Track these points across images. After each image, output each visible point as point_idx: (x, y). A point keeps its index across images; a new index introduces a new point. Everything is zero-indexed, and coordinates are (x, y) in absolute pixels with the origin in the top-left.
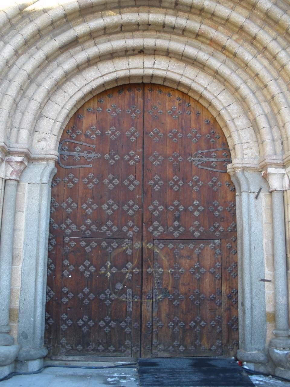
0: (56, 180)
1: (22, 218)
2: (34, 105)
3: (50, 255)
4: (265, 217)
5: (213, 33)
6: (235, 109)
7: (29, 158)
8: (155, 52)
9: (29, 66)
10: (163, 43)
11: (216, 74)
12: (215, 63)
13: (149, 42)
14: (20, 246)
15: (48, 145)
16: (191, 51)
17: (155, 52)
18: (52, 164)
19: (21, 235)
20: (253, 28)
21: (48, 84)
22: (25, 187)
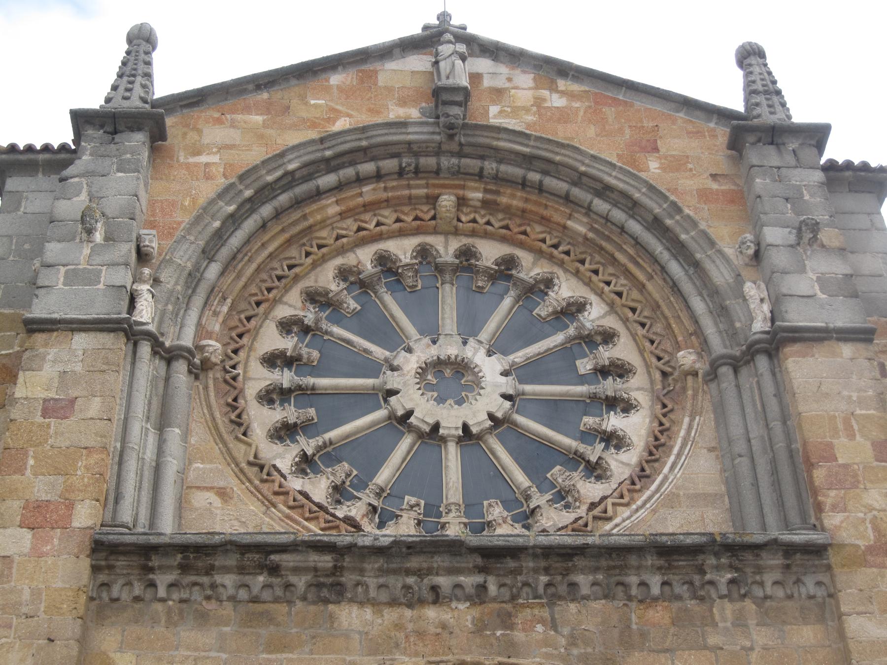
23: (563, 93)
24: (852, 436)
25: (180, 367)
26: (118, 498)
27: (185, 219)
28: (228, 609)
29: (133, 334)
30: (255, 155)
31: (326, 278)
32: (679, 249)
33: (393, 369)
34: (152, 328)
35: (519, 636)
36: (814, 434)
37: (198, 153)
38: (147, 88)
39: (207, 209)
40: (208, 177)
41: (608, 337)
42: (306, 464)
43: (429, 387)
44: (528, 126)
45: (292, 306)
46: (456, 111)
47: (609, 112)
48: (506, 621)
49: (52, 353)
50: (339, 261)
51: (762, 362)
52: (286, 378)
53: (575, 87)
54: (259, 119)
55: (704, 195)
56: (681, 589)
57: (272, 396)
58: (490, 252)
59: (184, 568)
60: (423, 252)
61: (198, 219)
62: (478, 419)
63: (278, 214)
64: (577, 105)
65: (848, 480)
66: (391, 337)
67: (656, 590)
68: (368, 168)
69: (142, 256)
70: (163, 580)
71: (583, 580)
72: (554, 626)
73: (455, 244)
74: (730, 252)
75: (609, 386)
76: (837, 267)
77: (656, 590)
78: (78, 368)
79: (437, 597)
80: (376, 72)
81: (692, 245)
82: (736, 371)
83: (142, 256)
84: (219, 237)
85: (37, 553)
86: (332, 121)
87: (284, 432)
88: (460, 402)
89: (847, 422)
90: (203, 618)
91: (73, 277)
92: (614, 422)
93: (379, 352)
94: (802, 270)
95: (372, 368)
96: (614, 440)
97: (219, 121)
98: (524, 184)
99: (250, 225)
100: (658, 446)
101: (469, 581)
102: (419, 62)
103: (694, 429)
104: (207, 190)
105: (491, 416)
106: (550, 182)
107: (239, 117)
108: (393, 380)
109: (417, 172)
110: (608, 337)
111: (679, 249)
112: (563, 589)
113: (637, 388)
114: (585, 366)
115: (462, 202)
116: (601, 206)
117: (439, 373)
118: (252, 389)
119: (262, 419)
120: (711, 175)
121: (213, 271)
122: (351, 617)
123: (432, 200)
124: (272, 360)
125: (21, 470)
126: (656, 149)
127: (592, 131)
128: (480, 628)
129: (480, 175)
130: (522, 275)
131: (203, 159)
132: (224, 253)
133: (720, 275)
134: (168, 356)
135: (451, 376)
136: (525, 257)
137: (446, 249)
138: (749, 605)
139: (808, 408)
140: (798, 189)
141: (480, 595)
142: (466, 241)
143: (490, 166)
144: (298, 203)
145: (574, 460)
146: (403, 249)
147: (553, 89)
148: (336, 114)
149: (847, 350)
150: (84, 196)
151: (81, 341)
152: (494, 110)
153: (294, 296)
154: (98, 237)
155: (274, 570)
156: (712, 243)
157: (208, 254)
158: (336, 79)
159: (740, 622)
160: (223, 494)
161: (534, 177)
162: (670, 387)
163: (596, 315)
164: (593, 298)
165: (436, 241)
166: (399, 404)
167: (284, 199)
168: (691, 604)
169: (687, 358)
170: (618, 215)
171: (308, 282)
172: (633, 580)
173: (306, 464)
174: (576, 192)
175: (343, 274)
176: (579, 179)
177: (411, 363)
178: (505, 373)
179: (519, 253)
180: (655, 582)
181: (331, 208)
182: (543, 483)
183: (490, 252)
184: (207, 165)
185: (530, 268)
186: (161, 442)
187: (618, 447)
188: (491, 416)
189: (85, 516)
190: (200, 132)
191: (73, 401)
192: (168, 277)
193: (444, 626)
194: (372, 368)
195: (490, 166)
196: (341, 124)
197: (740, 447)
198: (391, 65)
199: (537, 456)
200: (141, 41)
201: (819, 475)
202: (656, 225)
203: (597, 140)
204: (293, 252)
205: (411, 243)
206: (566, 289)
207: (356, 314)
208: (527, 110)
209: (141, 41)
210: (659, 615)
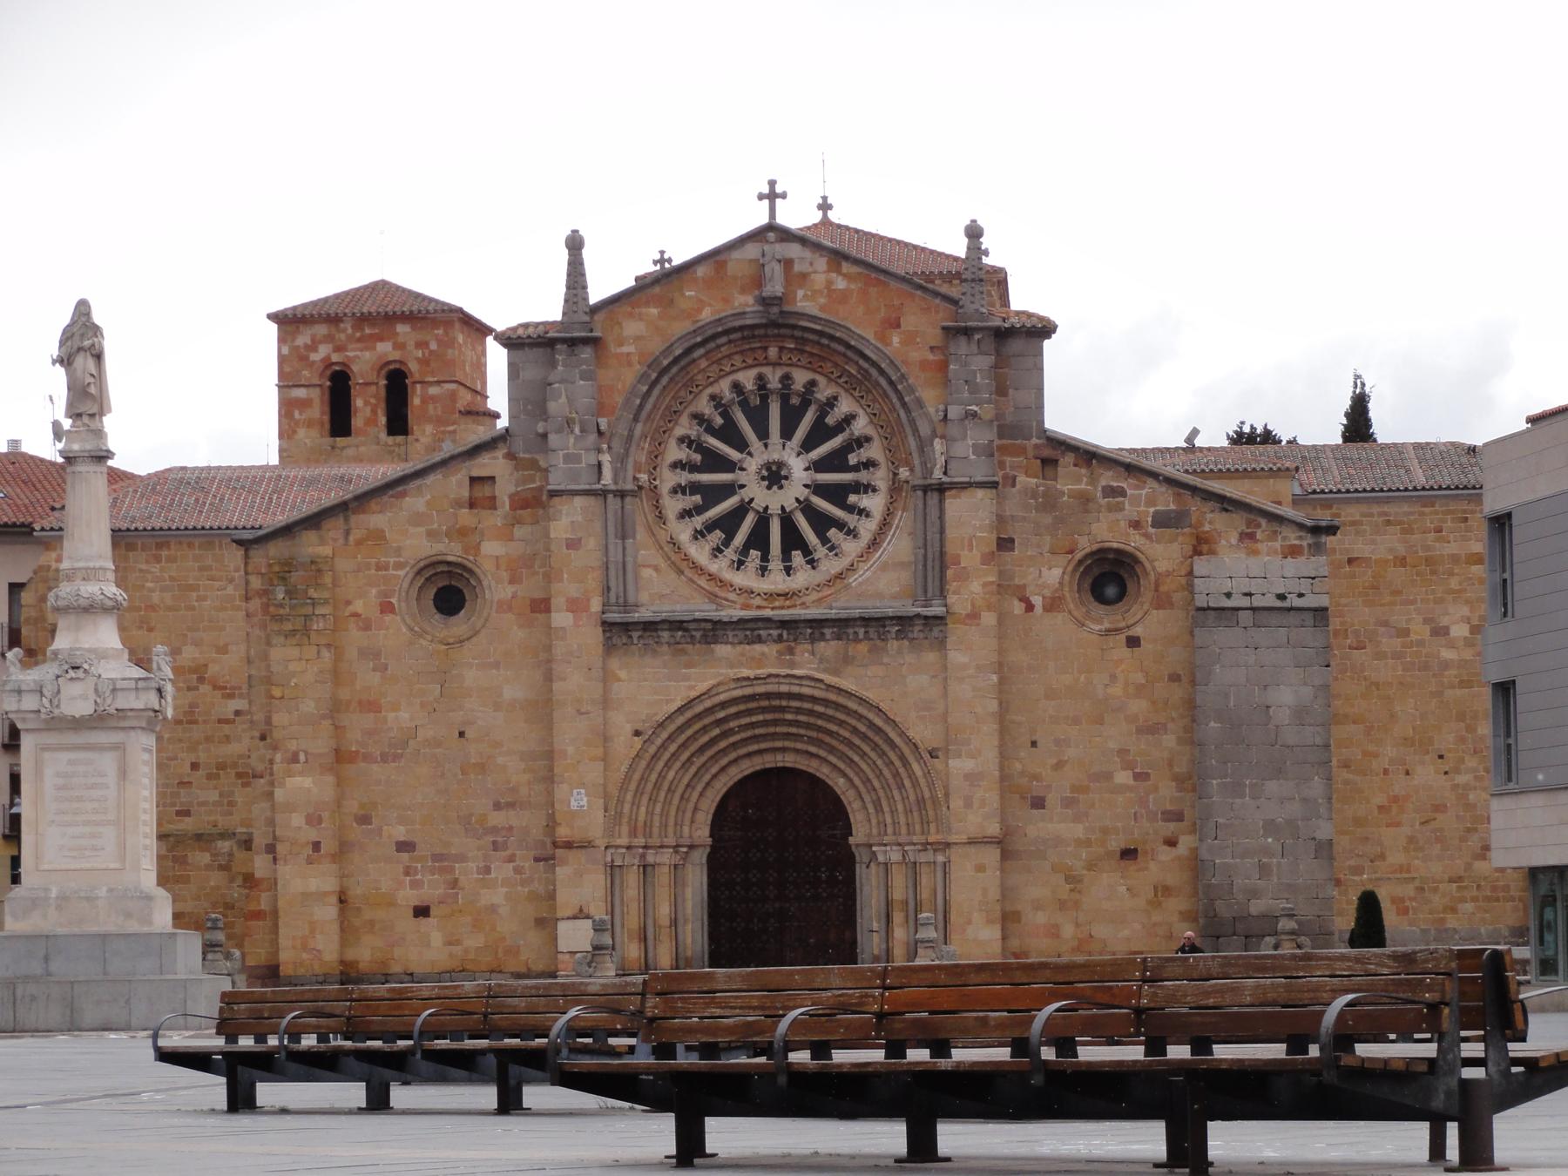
0: (711, 859)
1: (689, 893)
2: (691, 806)
3: (710, 916)
4: (874, 883)
5: (828, 739)
6: (851, 793)
7: (691, 847)
8: (783, 750)
9: (685, 781)
10: (787, 744)
11: (835, 766)
12: (832, 759)
13: (779, 744)
14: (689, 911)
15: (703, 833)
16: (813, 749)
17: (783, 750)
18: (708, 850)
19: (689, 904)
20: (857, 741)
21: (699, 788)
22: (689, 867)
23: (845, 276)
24: (971, 550)
25: (628, 499)
26: (609, 589)
27: (619, 400)
28: (665, 648)
29: (603, 494)
30: (656, 346)
31: (704, 406)
32: (904, 405)
33: (742, 469)
34: (613, 487)
35: (797, 658)
36: (950, 549)
37: (621, 345)
38: (586, 299)
39: (632, 392)
40: (630, 364)
41: (868, 439)
42: (698, 535)
43: (763, 478)
44: (822, 309)
45: (685, 427)
46: (775, 310)
47: (873, 291)
48: (791, 651)
49: (565, 509)
50: (709, 391)
51: (936, 495)
52: (684, 477)
53: (855, 269)
54: (654, 311)
55: (924, 365)
56: (873, 634)
57: (678, 490)
58: (800, 378)
59: (645, 630)
60: (760, 377)
61: (627, 401)
62: (790, 505)
63: (671, 379)
64: (853, 286)
65: (964, 576)
66: (741, 445)
67: (861, 636)
68: (724, 340)
69: (600, 433)
70: (635, 635)
71: (828, 632)
72: (813, 653)
73: (779, 373)
74: (931, 410)
75: (863, 476)
76: (986, 436)
77: (861, 636)
78: (580, 518)
79: (759, 640)
80: (725, 262)
81: (912, 406)
82: (925, 492)
83: (600, 433)
84: (641, 407)
85: (576, 625)
86: (699, 311)
87: (686, 514)
88: (781, 487)
89: (970, 541)
90: (655, 651)
91: (567, 458)
92: (865, 501)
93: (734, 455)
94: (965, 438)
95: (730, 466)
96: (863, 512)
97: (631, 315)
98: (818, 343)
99: (656, 392)
100: (885, 525)
101: (775, 633)
102: (752, 251)
103: (902, 519)
104: (629, 376)
105: (797, 500)
106: (834, 345)
107: (644, 310)
108: (742, 477)
109: (754, 337)
110: (868, 439)
111: (904, 405)
112: (817, 634)
113: (880, 478)
114: (853, 459)
115: (781, 349)
116: (861, 362)
117: (769, 469)
118: (665, 489)
119: (672, 506)
120: (932, 348)
121: (639, 428)
122: (722, 650)
123: (765, 349)
124: (676, 465)
125: (561, 580)
126: (898, 326)
127: (861, 310)
128: (780, 653)
129: (792, 337)
130: (818, 396)
131: (625, 349)
132: (644, 414)
133: (925, 430)
134: (622, 494)
135: (775, 476)
136: (821, 380)
137: (774, 378)
138: (906, 642)
139: (950, 533)
140: (974, 372)
141: (780, 639)
142: (786, 369)
143: (798, 333)
144: (682, 369)
145: (841, 525)
146: (747, 379)
147: (839, 272)
148: (701, 305)
149: (980, 493)
150: (563, 399)
151: (579, 501)
152: (800, 293)
153: (684, 419)
154: (577, 430)
155: (686, 630)
156: (920, 403)
157: (636, 419)
158: (701, 271)
159: (900, 652)
160: (656, 569)
161: (825, 341)
162: (896, 488)
163: (861, 426)
164: (861, 412)
165: (767, 370)
166: (745, 494)
167: (674, 370)
168: (878, 642)
169: (904, 473)
170: (874, 372)
171: (692, 409)
172: (851, 631)
173: (698, 535)
174: (849, 353)
175: (713, 397)
176: (849, 346)
177: (753, 465)
178: (807, 469)
179: (819, 378)
180: (861, 631)
181: (703, 364)
182: (824, 540)
183: (800, 378)
184: (628, 354)
185: (824, 391)
186: (624, 549)
187: (868, 515)
188: (797, 500)
189: (596, 605)
190: (620, 324)
191: (580, 540)
192: (616, 444)
193: (763, 654)
194: (730, 466)
195: (798, 333)
196: (707, 315)
197: (920, 544)
198: (736, 255)
199: (822, 523)
200: (575, 244)
201: (950, 573)
202: (891, 383)
203: (860, 324)
204: (682, 393)
205: (753, 373)
206: (845, 406)
207: (722, 427)
208: (820, 292)
209: (575, 244)
210: (863, 647)
